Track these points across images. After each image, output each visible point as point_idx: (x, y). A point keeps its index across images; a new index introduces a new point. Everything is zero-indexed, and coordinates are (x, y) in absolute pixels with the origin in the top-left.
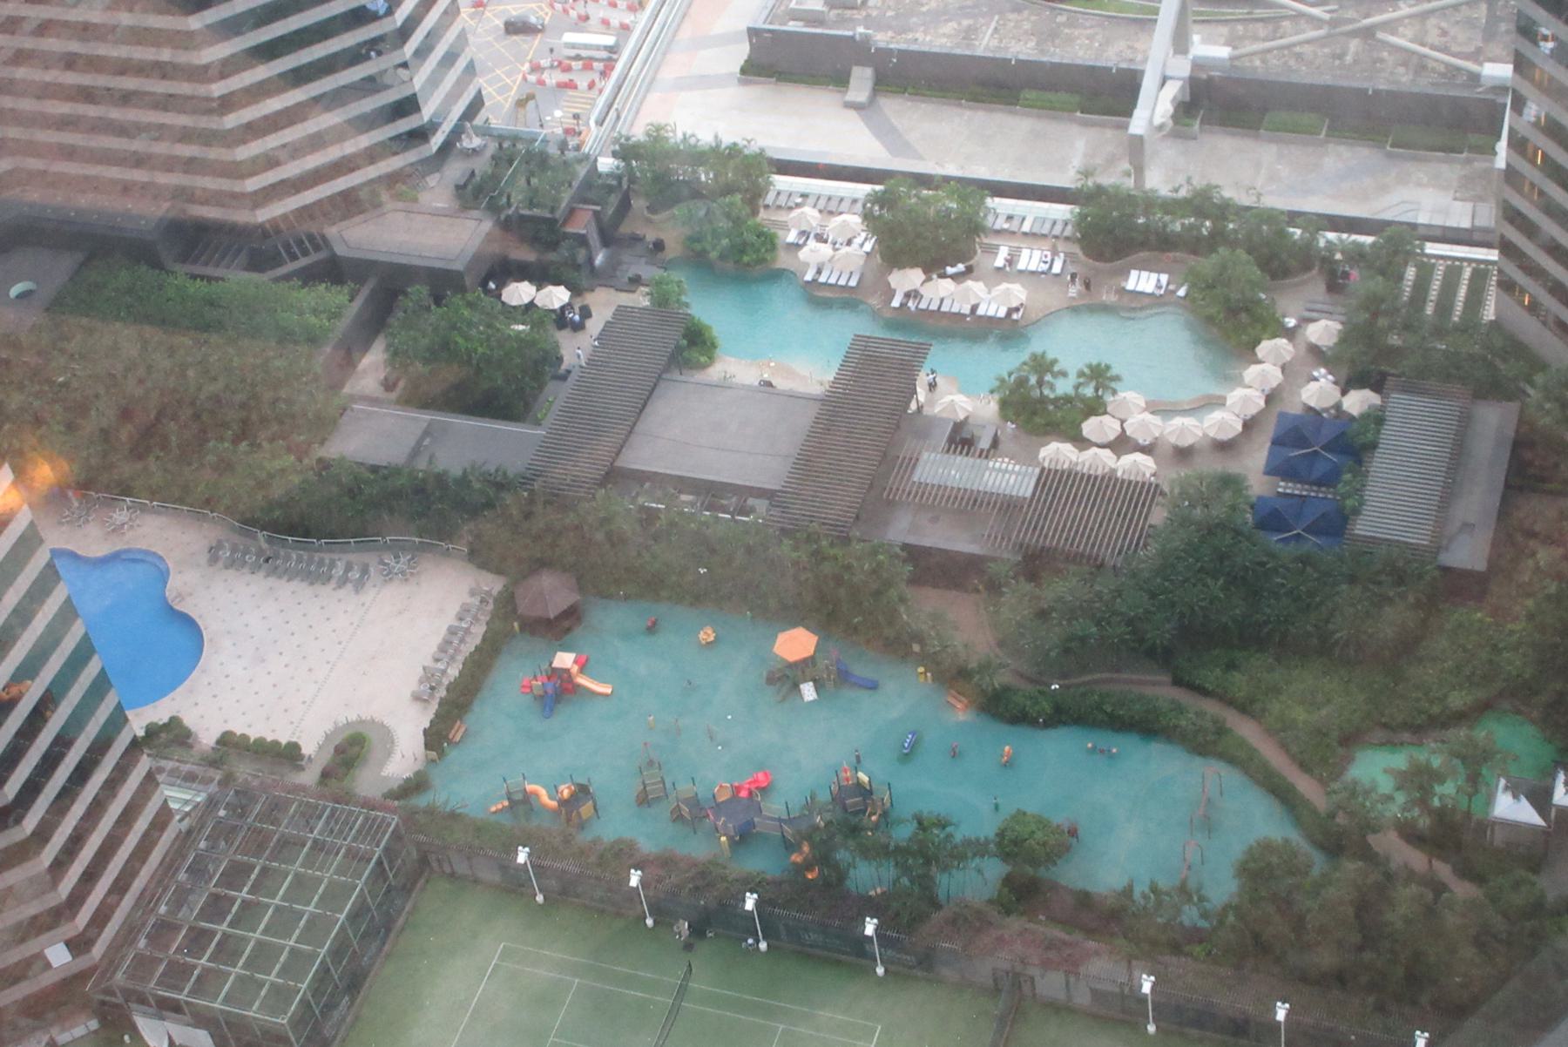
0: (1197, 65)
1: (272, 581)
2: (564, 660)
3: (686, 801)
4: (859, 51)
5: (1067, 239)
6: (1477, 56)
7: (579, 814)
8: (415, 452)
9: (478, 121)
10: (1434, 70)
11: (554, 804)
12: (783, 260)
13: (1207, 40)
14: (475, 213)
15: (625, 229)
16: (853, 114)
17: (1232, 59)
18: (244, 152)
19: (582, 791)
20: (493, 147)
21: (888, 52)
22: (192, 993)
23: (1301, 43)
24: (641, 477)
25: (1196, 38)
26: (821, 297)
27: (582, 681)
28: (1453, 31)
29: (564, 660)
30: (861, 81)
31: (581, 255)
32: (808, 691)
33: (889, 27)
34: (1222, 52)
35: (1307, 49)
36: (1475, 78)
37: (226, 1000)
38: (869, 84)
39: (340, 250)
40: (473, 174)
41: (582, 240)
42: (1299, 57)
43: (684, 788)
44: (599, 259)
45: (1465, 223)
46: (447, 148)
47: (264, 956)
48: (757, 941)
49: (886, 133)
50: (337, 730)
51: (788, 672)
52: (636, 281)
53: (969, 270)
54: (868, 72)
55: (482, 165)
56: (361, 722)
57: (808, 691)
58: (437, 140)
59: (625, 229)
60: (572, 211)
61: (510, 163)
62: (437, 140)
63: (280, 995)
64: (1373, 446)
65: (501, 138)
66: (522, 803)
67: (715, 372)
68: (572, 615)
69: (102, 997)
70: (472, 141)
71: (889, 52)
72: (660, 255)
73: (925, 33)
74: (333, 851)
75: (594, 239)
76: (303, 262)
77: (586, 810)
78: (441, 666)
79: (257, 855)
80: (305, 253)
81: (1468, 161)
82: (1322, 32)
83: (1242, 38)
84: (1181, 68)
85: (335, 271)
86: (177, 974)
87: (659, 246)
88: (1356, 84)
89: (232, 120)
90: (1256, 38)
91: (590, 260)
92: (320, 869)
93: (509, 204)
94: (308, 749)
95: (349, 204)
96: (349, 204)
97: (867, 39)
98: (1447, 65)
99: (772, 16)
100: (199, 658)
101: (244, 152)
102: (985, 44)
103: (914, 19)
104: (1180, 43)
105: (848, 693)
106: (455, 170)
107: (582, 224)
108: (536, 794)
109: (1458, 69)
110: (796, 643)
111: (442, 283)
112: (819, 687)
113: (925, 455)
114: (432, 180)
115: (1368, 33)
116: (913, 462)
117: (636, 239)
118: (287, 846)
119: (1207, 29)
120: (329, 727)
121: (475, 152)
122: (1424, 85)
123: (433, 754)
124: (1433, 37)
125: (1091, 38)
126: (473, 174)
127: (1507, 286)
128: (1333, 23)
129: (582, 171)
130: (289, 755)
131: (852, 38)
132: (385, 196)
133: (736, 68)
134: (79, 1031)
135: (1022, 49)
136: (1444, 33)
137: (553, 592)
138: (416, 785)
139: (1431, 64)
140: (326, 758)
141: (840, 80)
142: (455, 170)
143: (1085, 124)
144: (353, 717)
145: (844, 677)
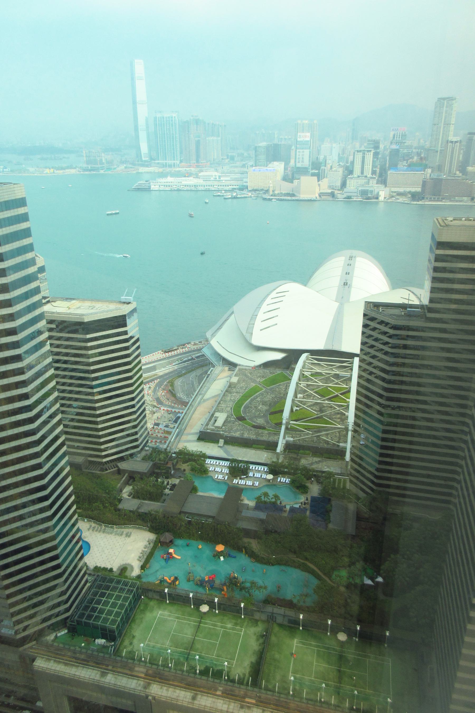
0: (287, 442)
1: (105, 534)
2: (171, 551)
3: (199, 580)
4: (221, 437)
5: (265, 472)
6: (338, 442)
7: (176, 584)
8: (138, 508)
9: (147, 445)
10: (330, 444)
11: (170, 581)
12: (210, 474)
13: (288, 437)
14: (149, 462)
15: (177, 467)
16: (220, 448)
17: (293, 440)
18: (103, 447)
19: (176, 579)
20: (151, 449)
21: (227, 437)
22: (93, 621)
23: (306, 438)
24: (185, 513)
25: (286, 436)
26: (218, 482)
27: (174, 555)
28: (333, 438)
29: (171, 551)
30: (222, 441)
31: (170, 471)
32: (222, 558)
33: (227, 432)
34: (292, 439)
35: (307, 439)
36: (338, 446)
37: (101, 622)
38: (223, 443)
39: (121, 468)
40: (147, 455)
41: (170, 468)
42: (305, 441)
43: (198, 578)
44: (172, 472)
45: (340, 472)
46: (142, 449)
47: (110, 613)
48: (216, 610)
49: (226, 452)
50: (121, 566)
51: (218, 554)
52: (180, 477)
53: (247, 477)
54: (223, 440)
55: (148, 453)
56: (126, 564)
57: (222, 558)
58: (141, 447)
59: (177, 467)
60: (167, 463)
61: (155, 452)
62: (141, 447)
63: (114, 621)
64: (331, 511)
65: (153, 448)
66: (162, 581)
67: (200, 493)
68: (171, 542)
69: (71, 623)
70: (147, 448)
71: (228, 437)
72: (185, 472)
73: (234, 433)
74: (124, 590)
75: (172, 468)
76: (112, 470)
77: (177, 583)
78: (146, 550)
79: (108, 590)
80: (115, 468)
81: (338, 461)
82: (310, 436)
83: (294, 437)
84: (284, 442)
85: (119, 472)
86: (90, 617)
87: (184, 470)
88: (316, 446)
89: (102, 440)
90: (297, 437)
91: (171, 472)
92: (122, 593)
93: (155, 460)
94: (115, 569)
95: (122, 459)
96: (122, 459)
97: (223, 434)
98: (333, 443)
99: (204, 429)
100: (89, 551)
101: (103, 447)
102: (246, 435)
103: (232, 431)
104: (284, 438)
105: (229, 558)
106: (143, 453)
107: (170, 465)
108: (166, 579)
109: (335, 444)
110: (220, 548)
111: (142, 476)
112: (224, 557)
113: (243, 511)
114: (139, 455)
115: (318, 436)
116: (241, 512)
117: (179, 469)
118: (115, 589)
119: (288, 435)
120: (119, 565)
121: (148, 450)
122: (329, 446)
123: (142, 571)
124: (330, 438)
125: (266, 436)
126: (147, 455)
127: (351, 481)
128: (312, 434)
129: (170, 454)
130: (111, 570)
131: (220, 434)
132: (129, 458)
133: (196, 439)
134: (63, 633)
135: (253, 437)
136: (331, 438)
137: (168, 536)
138: (139, 577)
139: (330, 443)
140: (119, 572)
141: (217, 442)
142: (143, 453)
143: (265, 451)
144: (124, 563)
145: (229, 556)
